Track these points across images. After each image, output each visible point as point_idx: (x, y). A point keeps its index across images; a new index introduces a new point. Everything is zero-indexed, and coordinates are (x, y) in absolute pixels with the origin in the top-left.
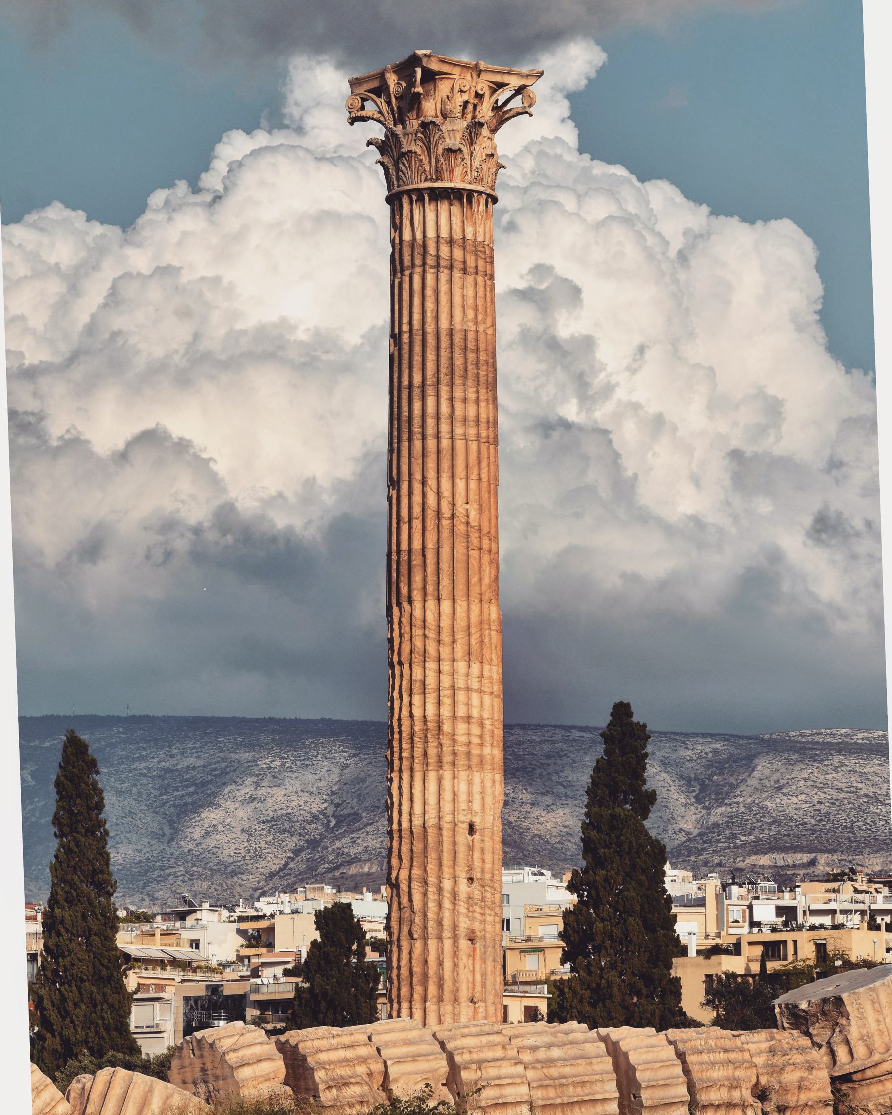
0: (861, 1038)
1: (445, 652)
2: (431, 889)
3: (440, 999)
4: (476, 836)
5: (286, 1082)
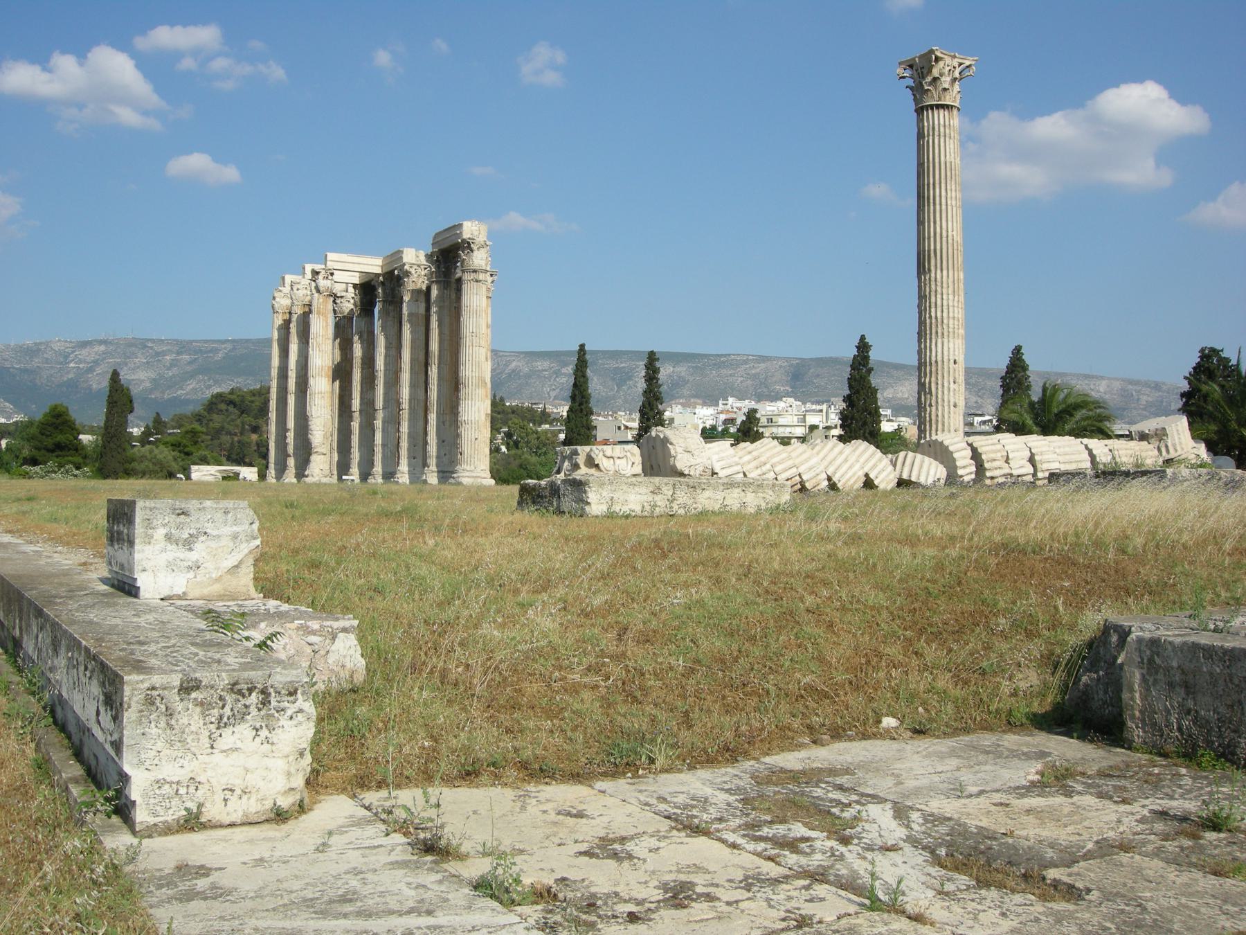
2: (940, 386)
5: (972, 458)
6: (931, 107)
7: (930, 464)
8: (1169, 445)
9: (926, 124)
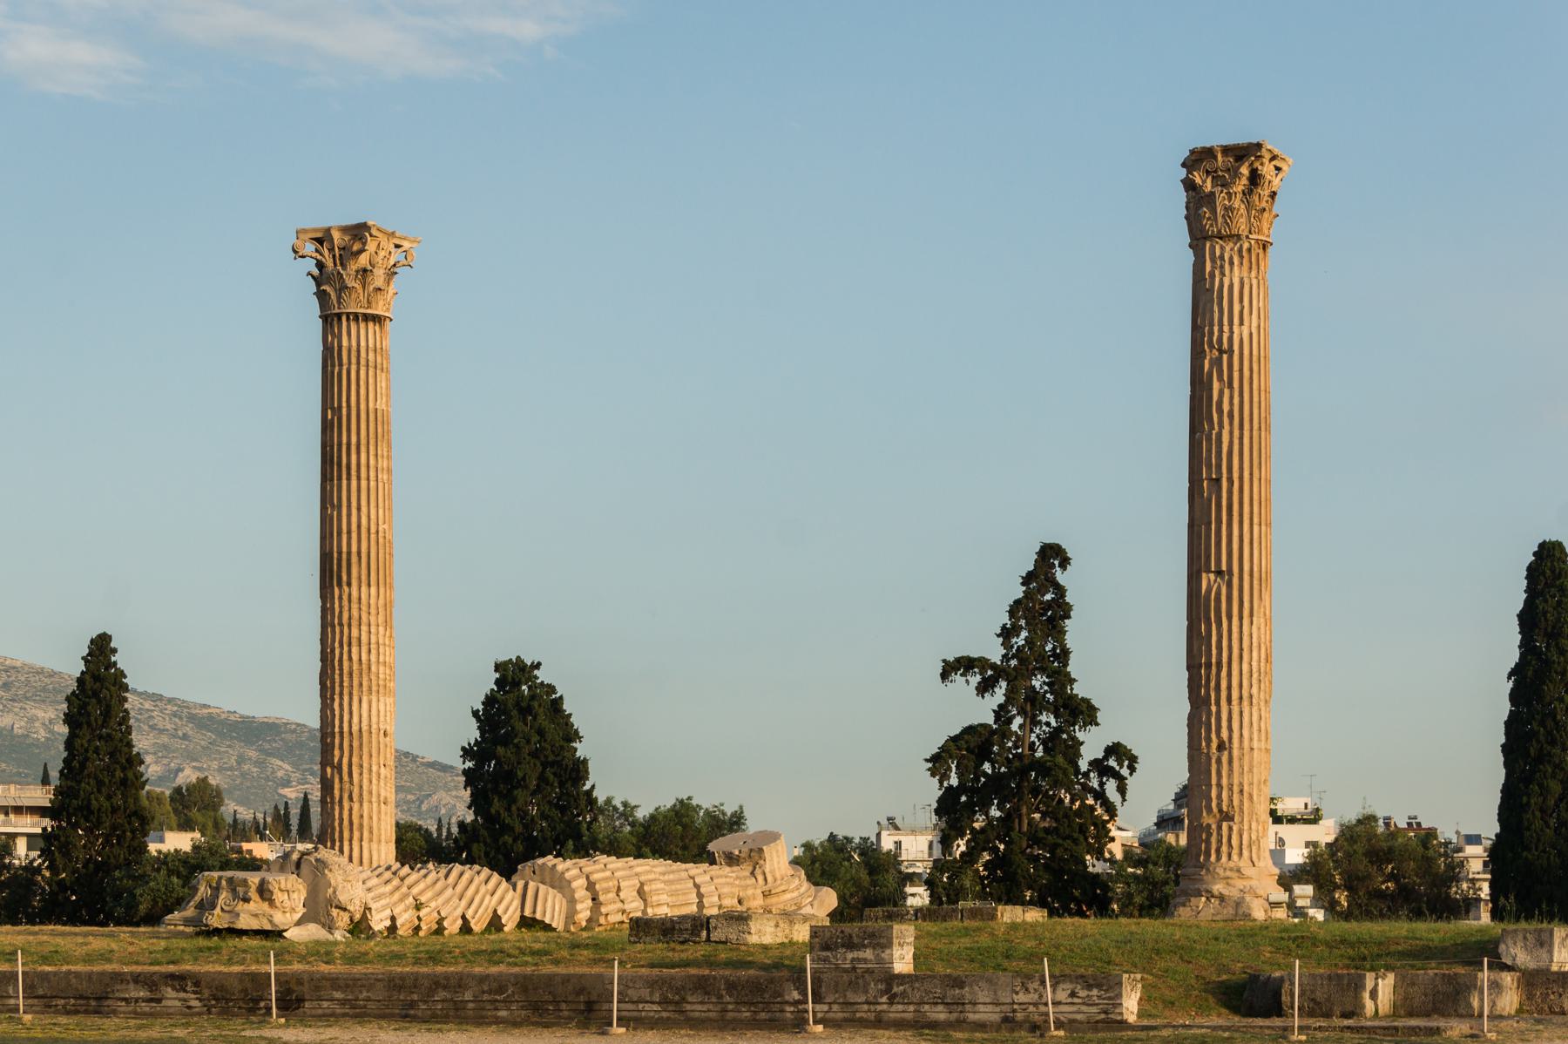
0: (770, 872)
2: (365, 771)
3: (371, 840)
4: (388, 738)
5: (587, 889)
7: (555, 897)
8: (767, 871)
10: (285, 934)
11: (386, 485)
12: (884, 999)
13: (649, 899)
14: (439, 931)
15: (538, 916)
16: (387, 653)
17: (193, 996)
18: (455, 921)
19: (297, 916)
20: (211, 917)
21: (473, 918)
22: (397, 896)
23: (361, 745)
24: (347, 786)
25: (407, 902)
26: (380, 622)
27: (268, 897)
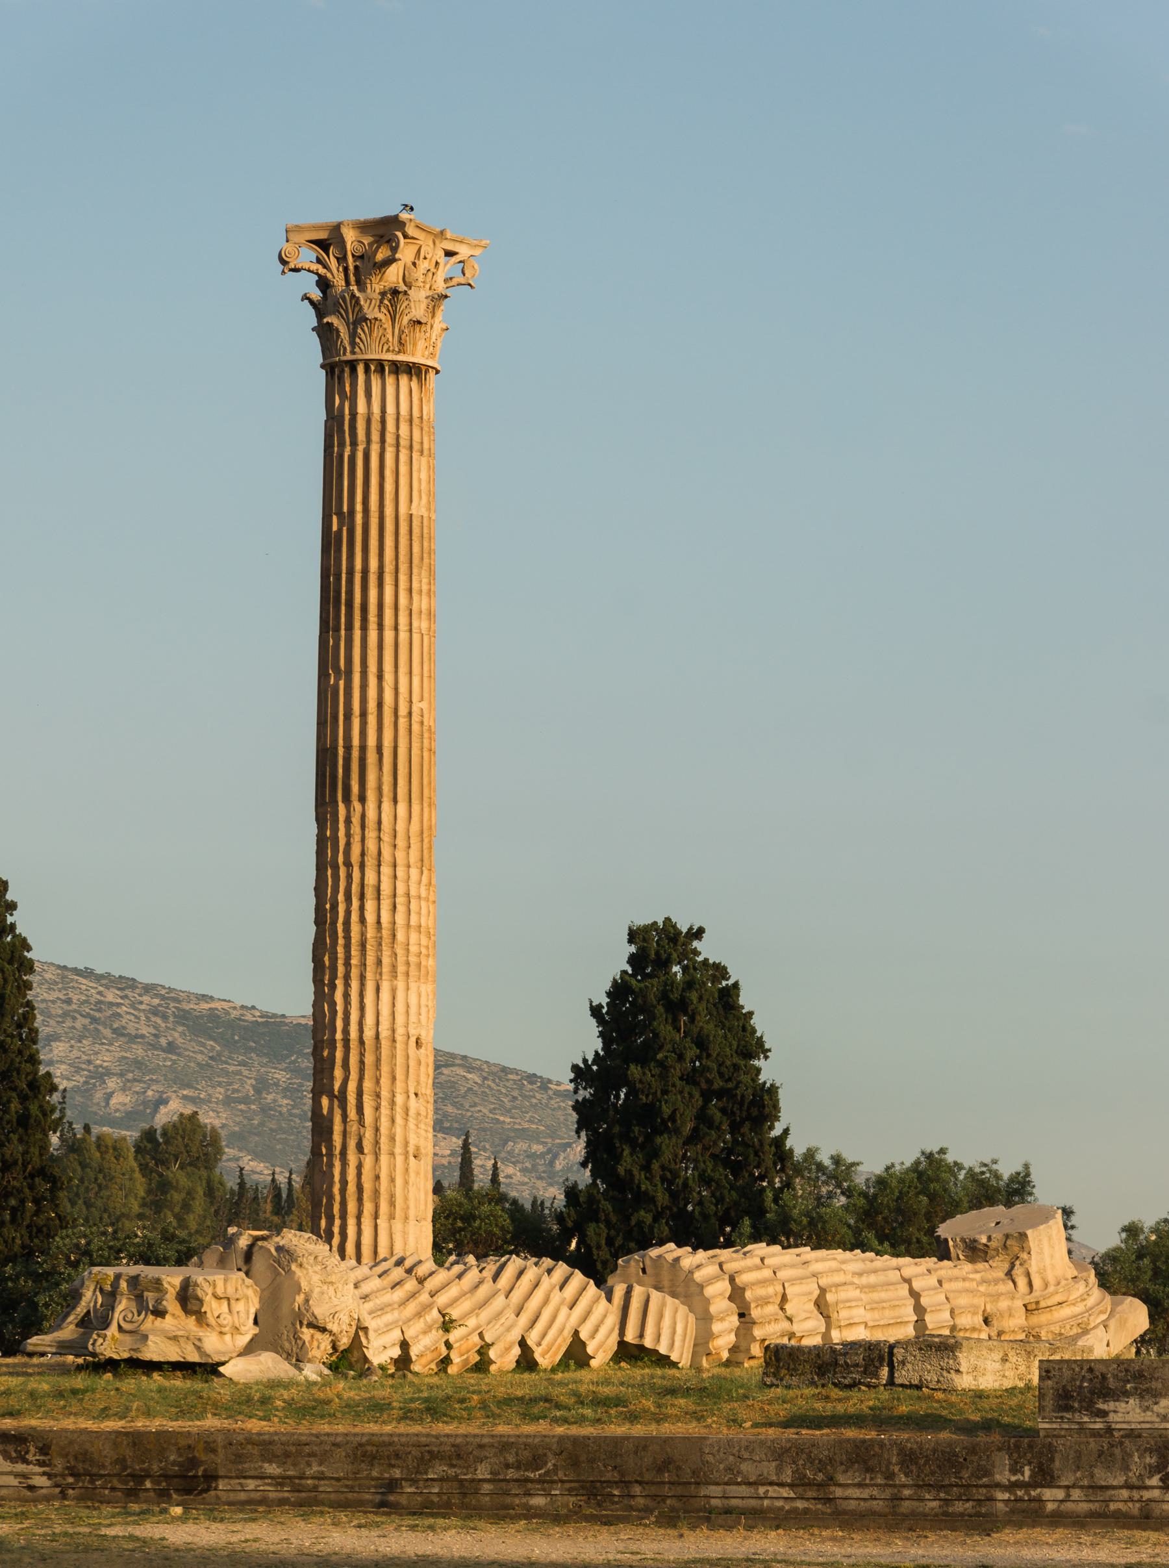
0: (1039, 1272)
1: (400, 856)
2: (384, 1103)
3: (392, 1217)
4: (422, 1050)
5: (730, 1298)
6: (380, 365)
7: (676, 1311)
8: (1033, 1270)
9: (361, 408)
10: (221, 1369)
11: (426, 638)
12: (1155, 1481)
13: (834, 1316)
14: (482, 1366)
15: (648, 1343)
16: (424, 911)
17: (38, 1469)
18: (508, 1349)
19: (244, 1340)
20: (100, 1341)
21: (539, 1344)
22: (412, 1307)
23: (378, 1060)
24: (353, 1128)
25: (428, 1318)
26: (412, 860)
27: (195, 1308)
